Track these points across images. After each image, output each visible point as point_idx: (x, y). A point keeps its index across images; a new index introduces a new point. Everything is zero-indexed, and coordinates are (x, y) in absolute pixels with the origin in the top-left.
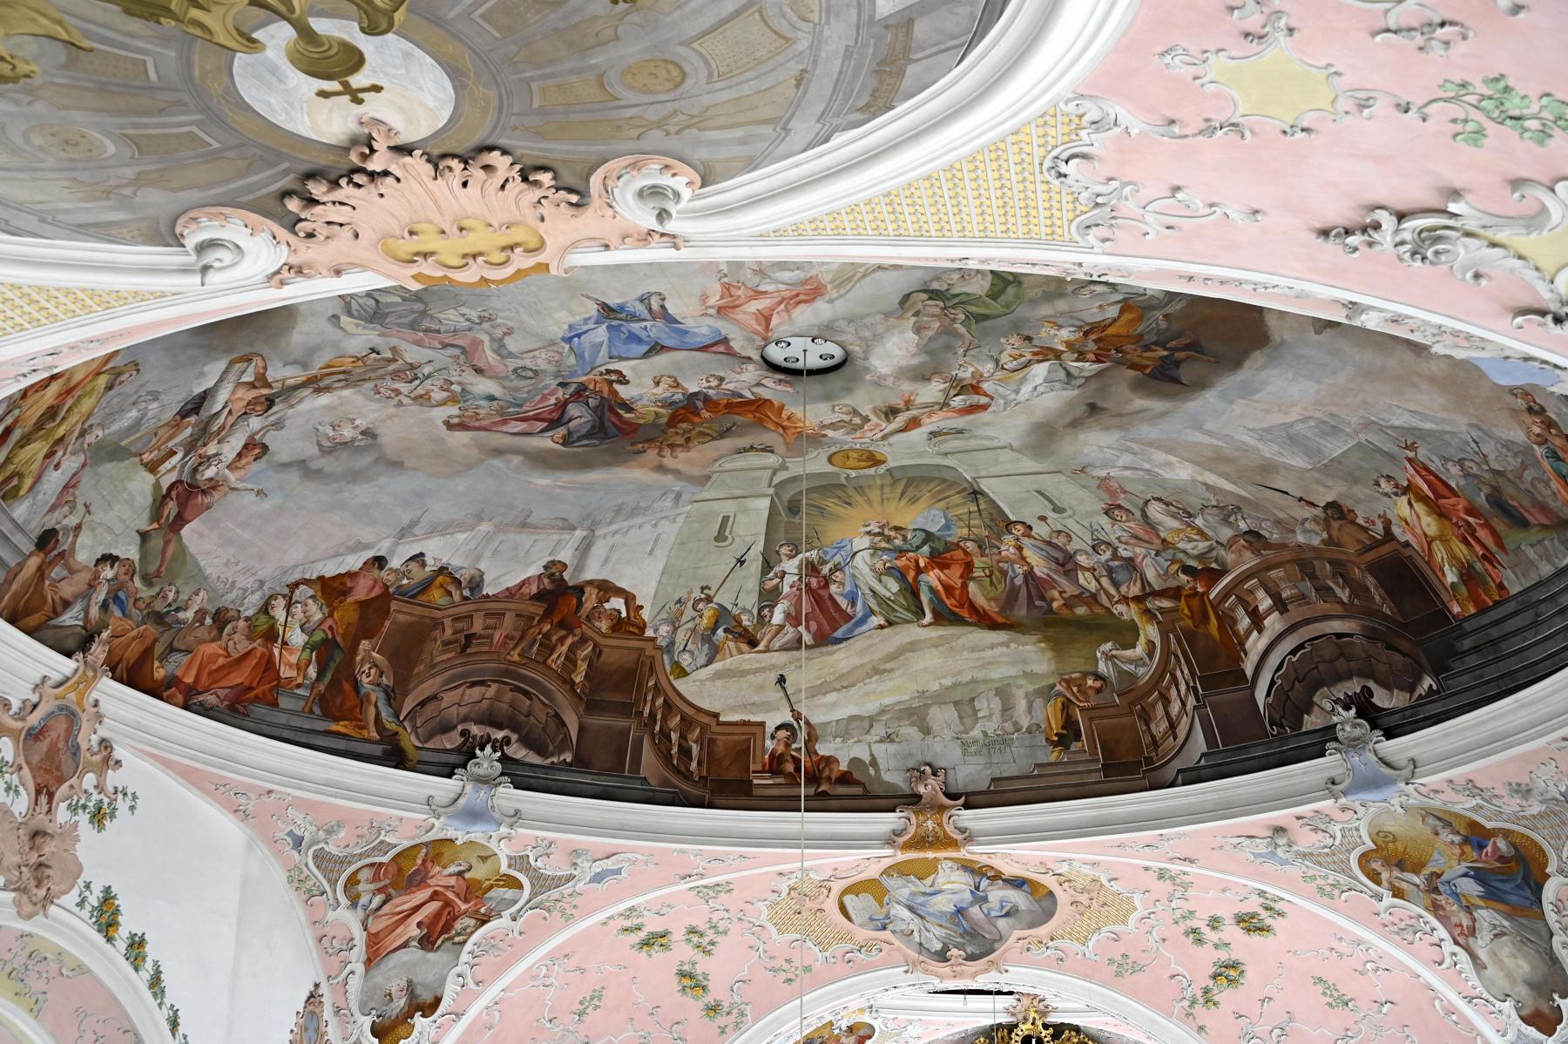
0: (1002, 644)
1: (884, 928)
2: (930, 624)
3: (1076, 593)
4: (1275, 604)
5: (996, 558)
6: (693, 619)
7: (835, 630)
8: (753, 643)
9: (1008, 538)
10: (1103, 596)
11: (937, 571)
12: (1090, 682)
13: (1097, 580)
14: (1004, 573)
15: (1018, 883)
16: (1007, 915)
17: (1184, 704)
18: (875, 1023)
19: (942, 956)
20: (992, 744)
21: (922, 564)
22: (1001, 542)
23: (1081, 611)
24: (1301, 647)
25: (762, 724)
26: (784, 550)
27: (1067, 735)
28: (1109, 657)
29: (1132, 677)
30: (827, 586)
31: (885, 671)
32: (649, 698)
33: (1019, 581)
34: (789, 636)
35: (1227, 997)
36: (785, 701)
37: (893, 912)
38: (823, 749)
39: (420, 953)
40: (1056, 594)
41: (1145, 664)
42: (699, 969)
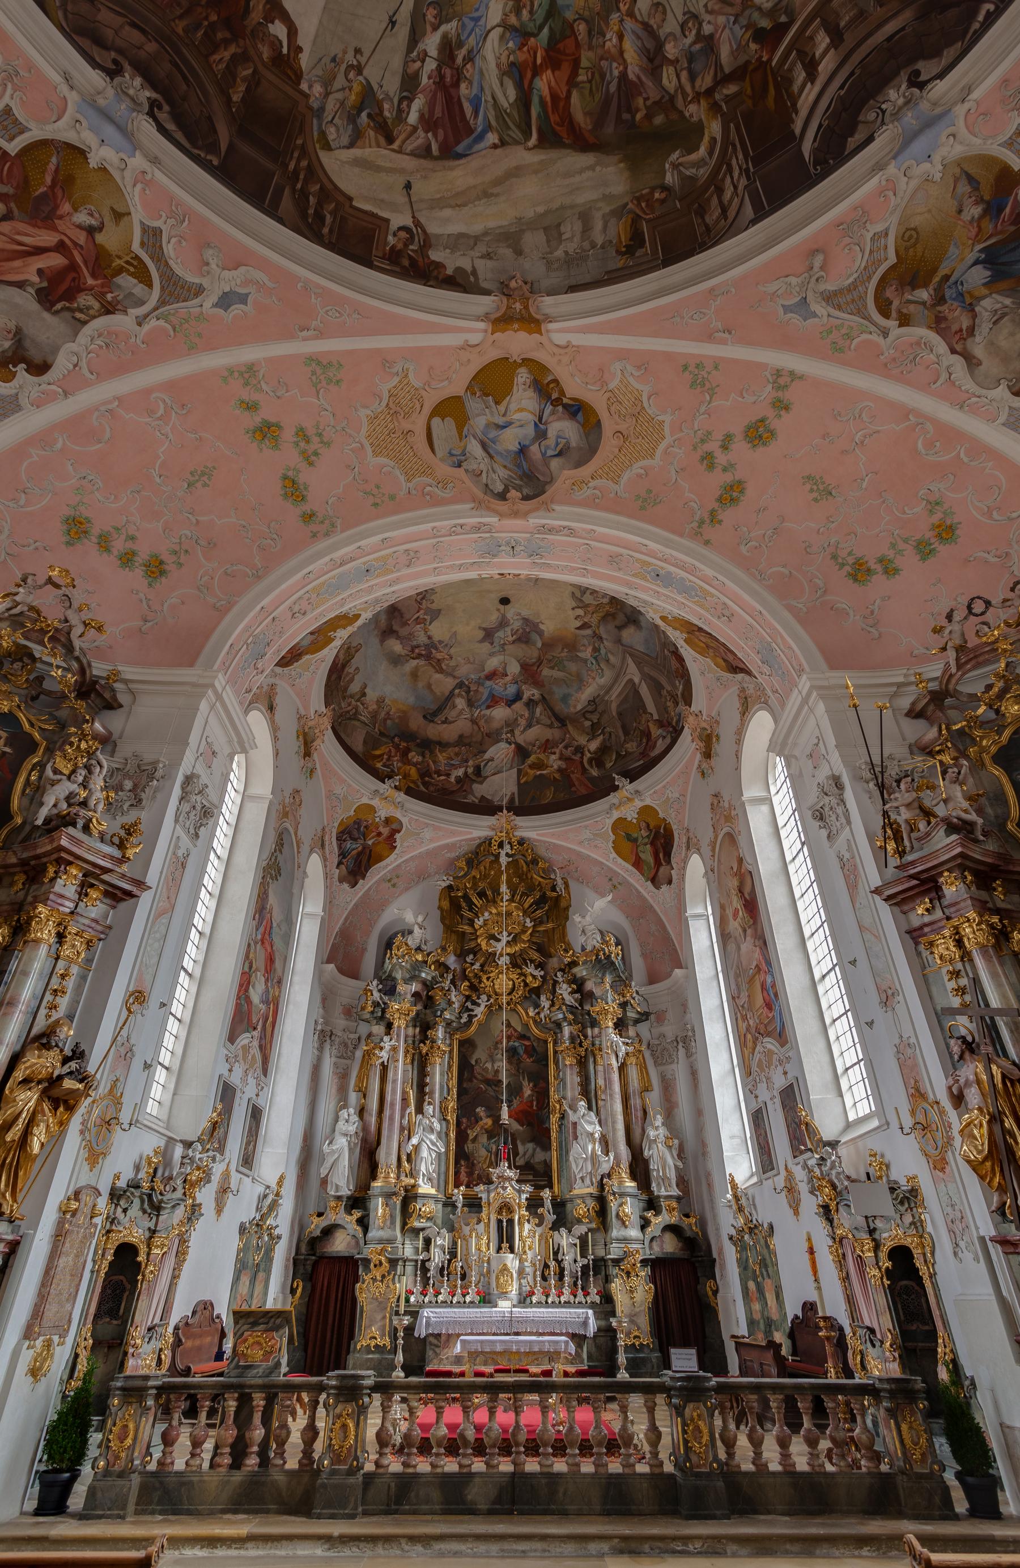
0: (592, 168)
1: (459, 466)
2: (535, 147)
3: (658, 98)
4: (832, 40)
5: (600, 52)
6: (343, 89)
7: (458, 142)
8: (390, 140)
9: (615, 17)
10: (680, 96)
11: (549, 72)
12: (657, 195)
13: (678, 76)
14: (603, 76)
15: (577, 409)
16: (560, 454)
17: (735, 187)
18: (405, 821)
19: (502, 496)
20: (569, 261)
21: (539, 61)
22: (607, 24)
23: (659, 120)
24: (852, 74)
25: (387, 221)
26: (430, 14)
27: (636, 239)
28: (675, 166)
29: (693, 179)
30: (456, 85)
31: (492, 195)
32: (296, 155)
33: (613, 88)
34: (420, 141)
35: (728, 516)
36: (408, 207)
37: (469, 448)
38: (435, 255)
39: (34, 306)
40: (640, 101)
41: (706, 164)
42: (302, 479)
